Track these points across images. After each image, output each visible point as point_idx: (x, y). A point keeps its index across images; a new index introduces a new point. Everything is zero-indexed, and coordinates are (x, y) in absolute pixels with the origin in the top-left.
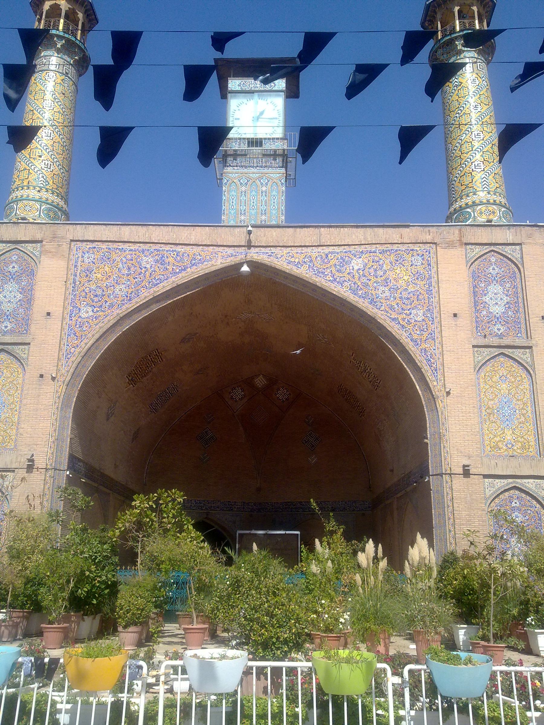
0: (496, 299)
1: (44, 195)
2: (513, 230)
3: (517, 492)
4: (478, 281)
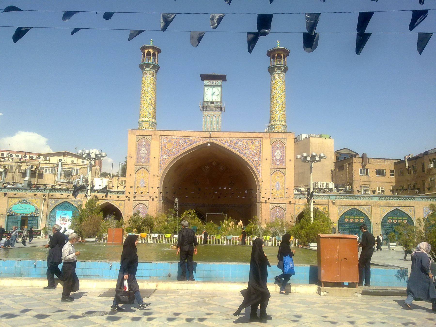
0: (278, 154)
1: (150, 119)
2: (284, 134)
4: (274, 148)
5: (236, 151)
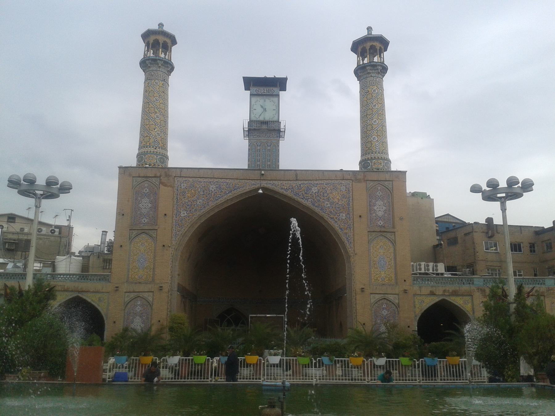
0: (380, 208)
3: (385, 301)
5: (308, 203)
